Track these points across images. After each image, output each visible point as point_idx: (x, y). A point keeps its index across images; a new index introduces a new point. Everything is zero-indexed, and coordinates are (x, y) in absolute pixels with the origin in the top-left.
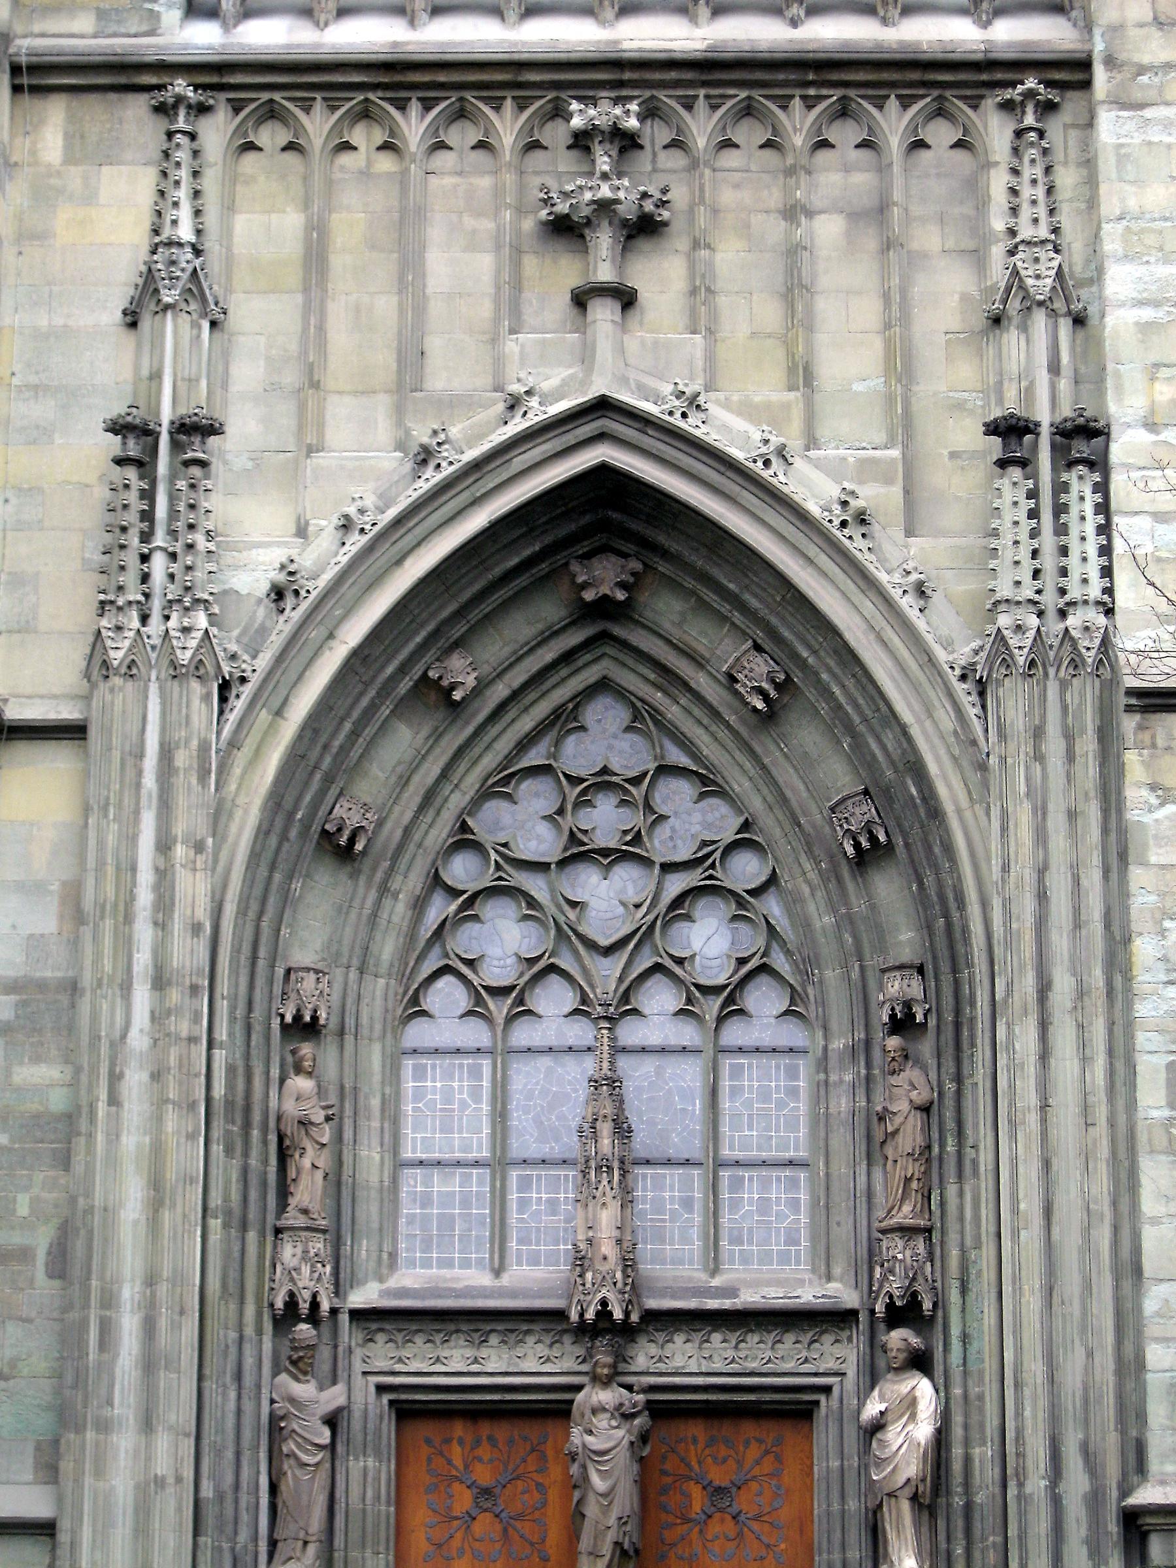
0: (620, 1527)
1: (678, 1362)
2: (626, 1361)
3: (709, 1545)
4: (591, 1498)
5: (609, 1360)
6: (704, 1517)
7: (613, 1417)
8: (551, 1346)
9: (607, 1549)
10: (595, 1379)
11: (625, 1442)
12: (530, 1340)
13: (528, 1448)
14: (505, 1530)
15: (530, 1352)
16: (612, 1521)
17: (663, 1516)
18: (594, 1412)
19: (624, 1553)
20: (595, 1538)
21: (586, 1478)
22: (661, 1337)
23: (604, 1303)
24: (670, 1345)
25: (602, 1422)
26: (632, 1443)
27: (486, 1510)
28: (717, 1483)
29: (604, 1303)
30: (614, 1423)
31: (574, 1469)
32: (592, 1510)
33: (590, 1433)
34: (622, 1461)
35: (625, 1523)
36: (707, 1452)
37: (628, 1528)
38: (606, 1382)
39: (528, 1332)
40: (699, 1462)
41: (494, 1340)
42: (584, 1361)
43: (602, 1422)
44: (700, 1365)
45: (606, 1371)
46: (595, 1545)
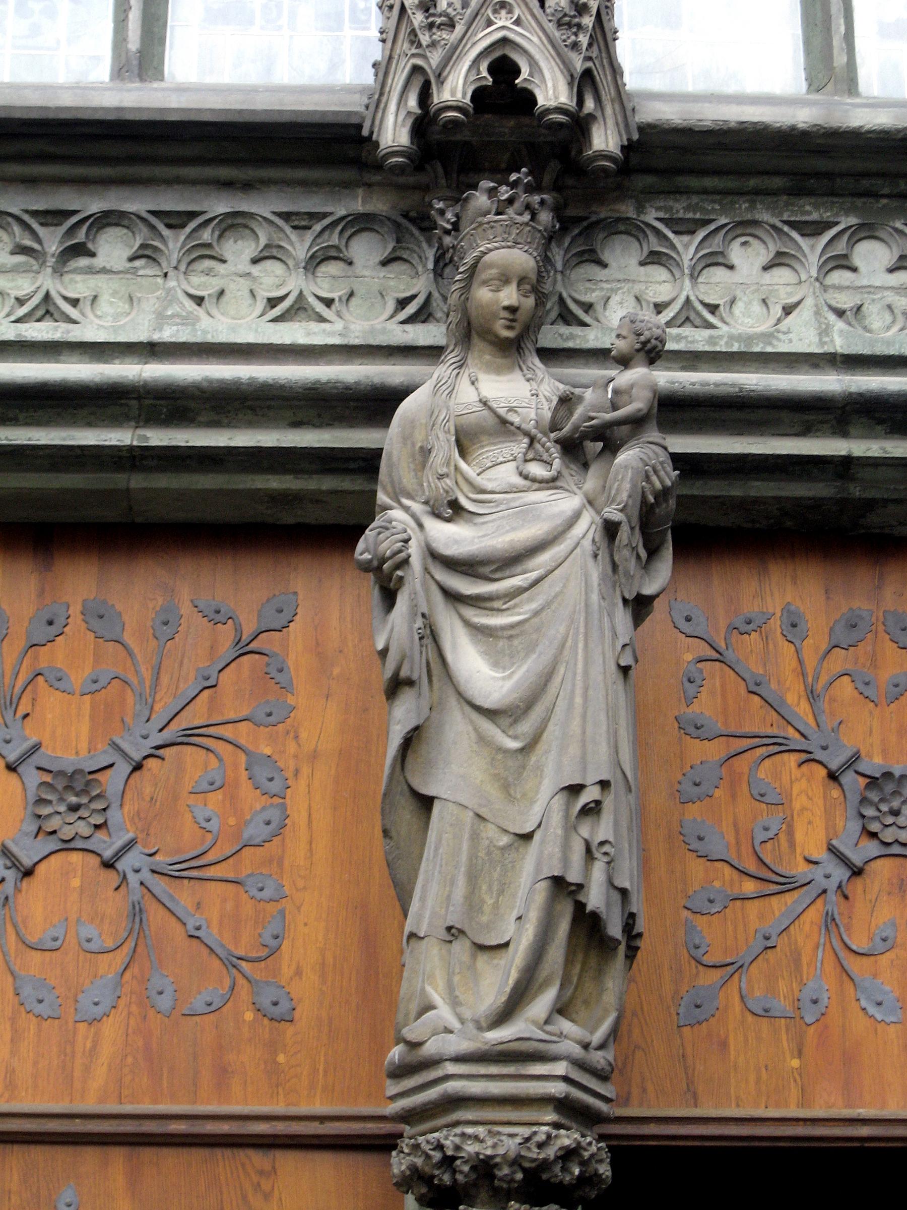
0: (570, 828)
1: (746, 323)
2: (567, 317)
3: (854, 965)
4: (458, 731)
5: (521, 259)
6: (840, 874)
7: (533, 452)
8: (314, 262)
9: (519, 916)
10: (470, 332)
11: (587, 526)
12: (239, 251)
13: (226, 649)
14: (137, 913)
15: (237, 289)
16: (541, 804)
17: (697, 869)
18: (464, 442)
19: (587, 925)
20: (473, 878)
21: (440, 665)
22: (688, 248)
23: (503, 68)
24: (719, 274)
25: (498, 468)
26: (610, 529)
27: (67, 845)
28: (874, 763)
29: (503, 68)
30: (537, 470)
31: (397, 627)
32: (458, 772)
33: (455, 511)
34: (574, 591)
35: (592, 810)
36: (839, 661)
37: (603, 830)
38: (515, 344)
39: (234, 224)
40: (812, 696)
41: (113, 249)
42: (423, 315)
43: (498, 468)
44: (825, 331)
45: (509, 295)
46: (472, 904)
